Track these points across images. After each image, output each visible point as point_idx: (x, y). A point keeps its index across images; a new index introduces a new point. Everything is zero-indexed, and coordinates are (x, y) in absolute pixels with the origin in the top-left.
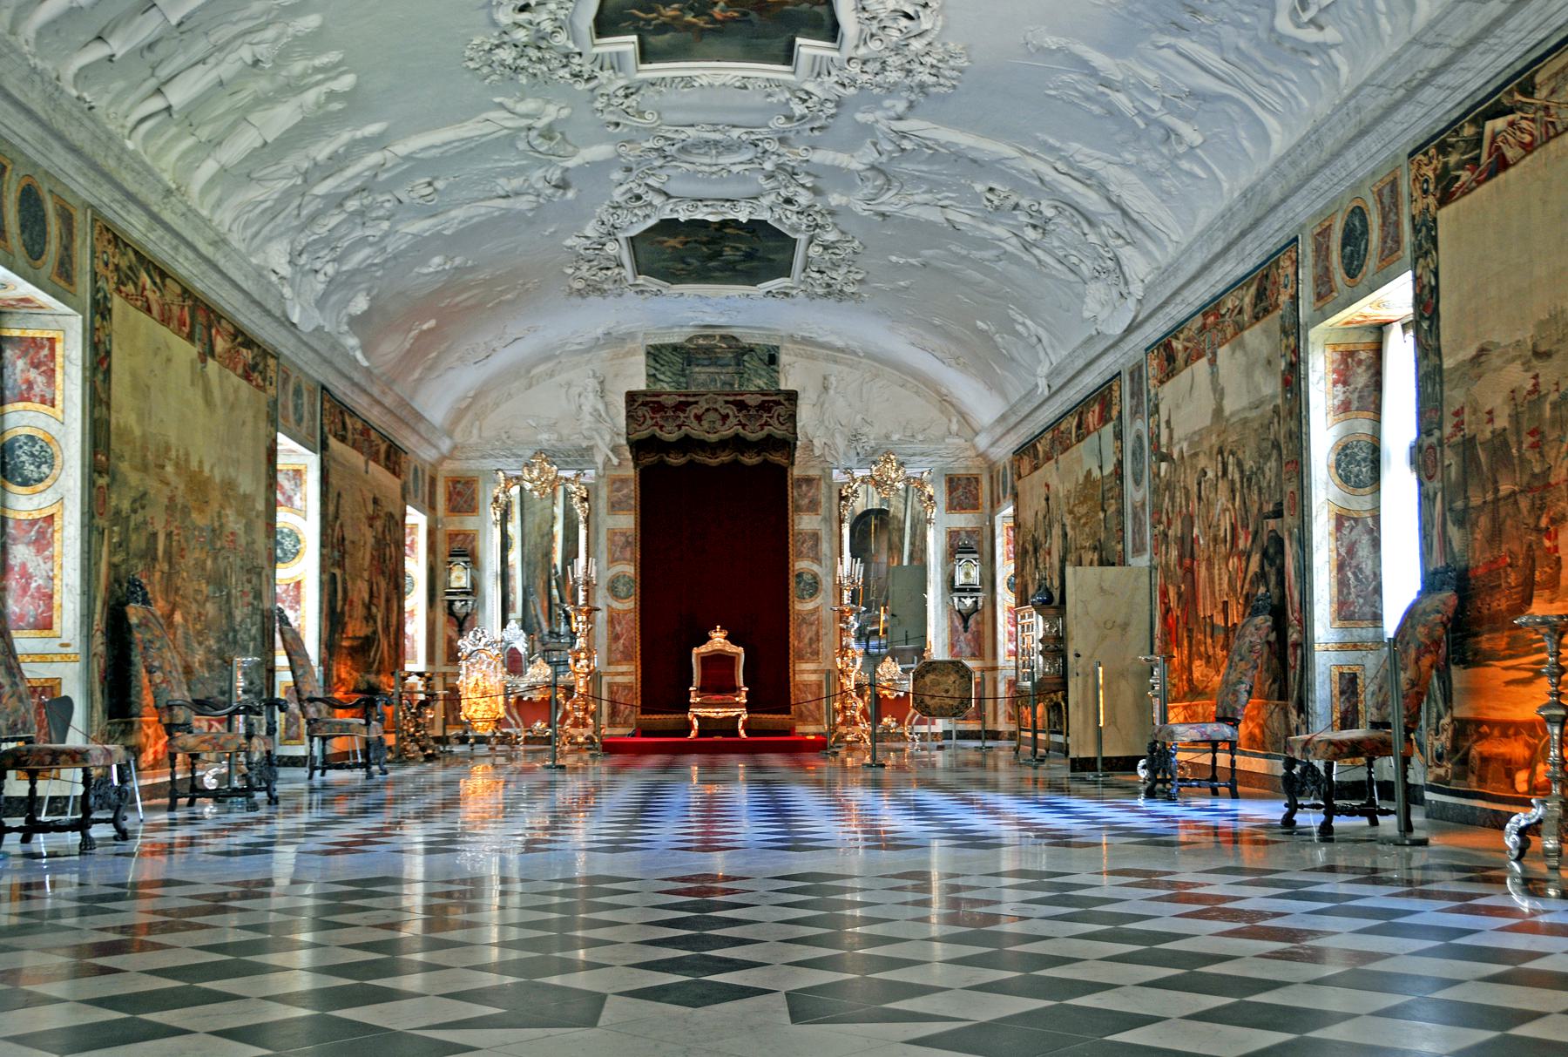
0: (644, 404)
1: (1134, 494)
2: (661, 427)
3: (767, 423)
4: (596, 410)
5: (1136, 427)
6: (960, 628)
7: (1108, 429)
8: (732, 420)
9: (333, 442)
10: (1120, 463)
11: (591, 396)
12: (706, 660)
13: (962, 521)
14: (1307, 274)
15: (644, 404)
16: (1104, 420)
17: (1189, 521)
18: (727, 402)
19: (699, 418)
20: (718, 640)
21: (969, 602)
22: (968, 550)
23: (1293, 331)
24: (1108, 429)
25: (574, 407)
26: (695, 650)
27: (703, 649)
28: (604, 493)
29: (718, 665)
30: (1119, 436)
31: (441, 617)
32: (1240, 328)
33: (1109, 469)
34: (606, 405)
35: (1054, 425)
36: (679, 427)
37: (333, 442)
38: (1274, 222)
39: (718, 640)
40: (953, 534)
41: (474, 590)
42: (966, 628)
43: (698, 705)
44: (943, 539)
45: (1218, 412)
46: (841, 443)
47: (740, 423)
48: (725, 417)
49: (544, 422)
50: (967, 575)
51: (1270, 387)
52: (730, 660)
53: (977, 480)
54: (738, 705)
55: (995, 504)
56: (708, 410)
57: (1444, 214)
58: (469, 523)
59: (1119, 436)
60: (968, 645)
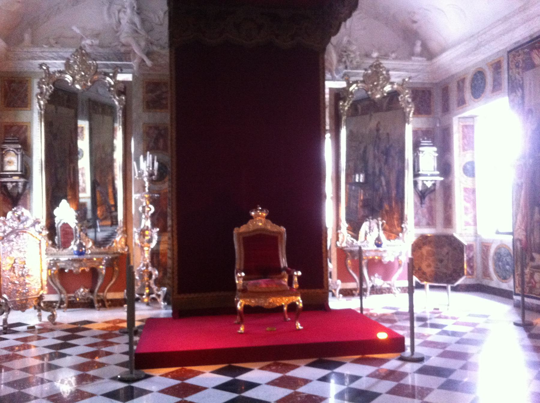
4: (134, 24)
6: (418, 204)
11: (129, 11)
20: (259, 219)
25: (114, 21)
26: (236, 231)
27: (243, 229)
29: (260, 243)
34: (143, 21)
39: (259, 219)
40: (415, 133)
41: (26, 172)
58: (22, 116)
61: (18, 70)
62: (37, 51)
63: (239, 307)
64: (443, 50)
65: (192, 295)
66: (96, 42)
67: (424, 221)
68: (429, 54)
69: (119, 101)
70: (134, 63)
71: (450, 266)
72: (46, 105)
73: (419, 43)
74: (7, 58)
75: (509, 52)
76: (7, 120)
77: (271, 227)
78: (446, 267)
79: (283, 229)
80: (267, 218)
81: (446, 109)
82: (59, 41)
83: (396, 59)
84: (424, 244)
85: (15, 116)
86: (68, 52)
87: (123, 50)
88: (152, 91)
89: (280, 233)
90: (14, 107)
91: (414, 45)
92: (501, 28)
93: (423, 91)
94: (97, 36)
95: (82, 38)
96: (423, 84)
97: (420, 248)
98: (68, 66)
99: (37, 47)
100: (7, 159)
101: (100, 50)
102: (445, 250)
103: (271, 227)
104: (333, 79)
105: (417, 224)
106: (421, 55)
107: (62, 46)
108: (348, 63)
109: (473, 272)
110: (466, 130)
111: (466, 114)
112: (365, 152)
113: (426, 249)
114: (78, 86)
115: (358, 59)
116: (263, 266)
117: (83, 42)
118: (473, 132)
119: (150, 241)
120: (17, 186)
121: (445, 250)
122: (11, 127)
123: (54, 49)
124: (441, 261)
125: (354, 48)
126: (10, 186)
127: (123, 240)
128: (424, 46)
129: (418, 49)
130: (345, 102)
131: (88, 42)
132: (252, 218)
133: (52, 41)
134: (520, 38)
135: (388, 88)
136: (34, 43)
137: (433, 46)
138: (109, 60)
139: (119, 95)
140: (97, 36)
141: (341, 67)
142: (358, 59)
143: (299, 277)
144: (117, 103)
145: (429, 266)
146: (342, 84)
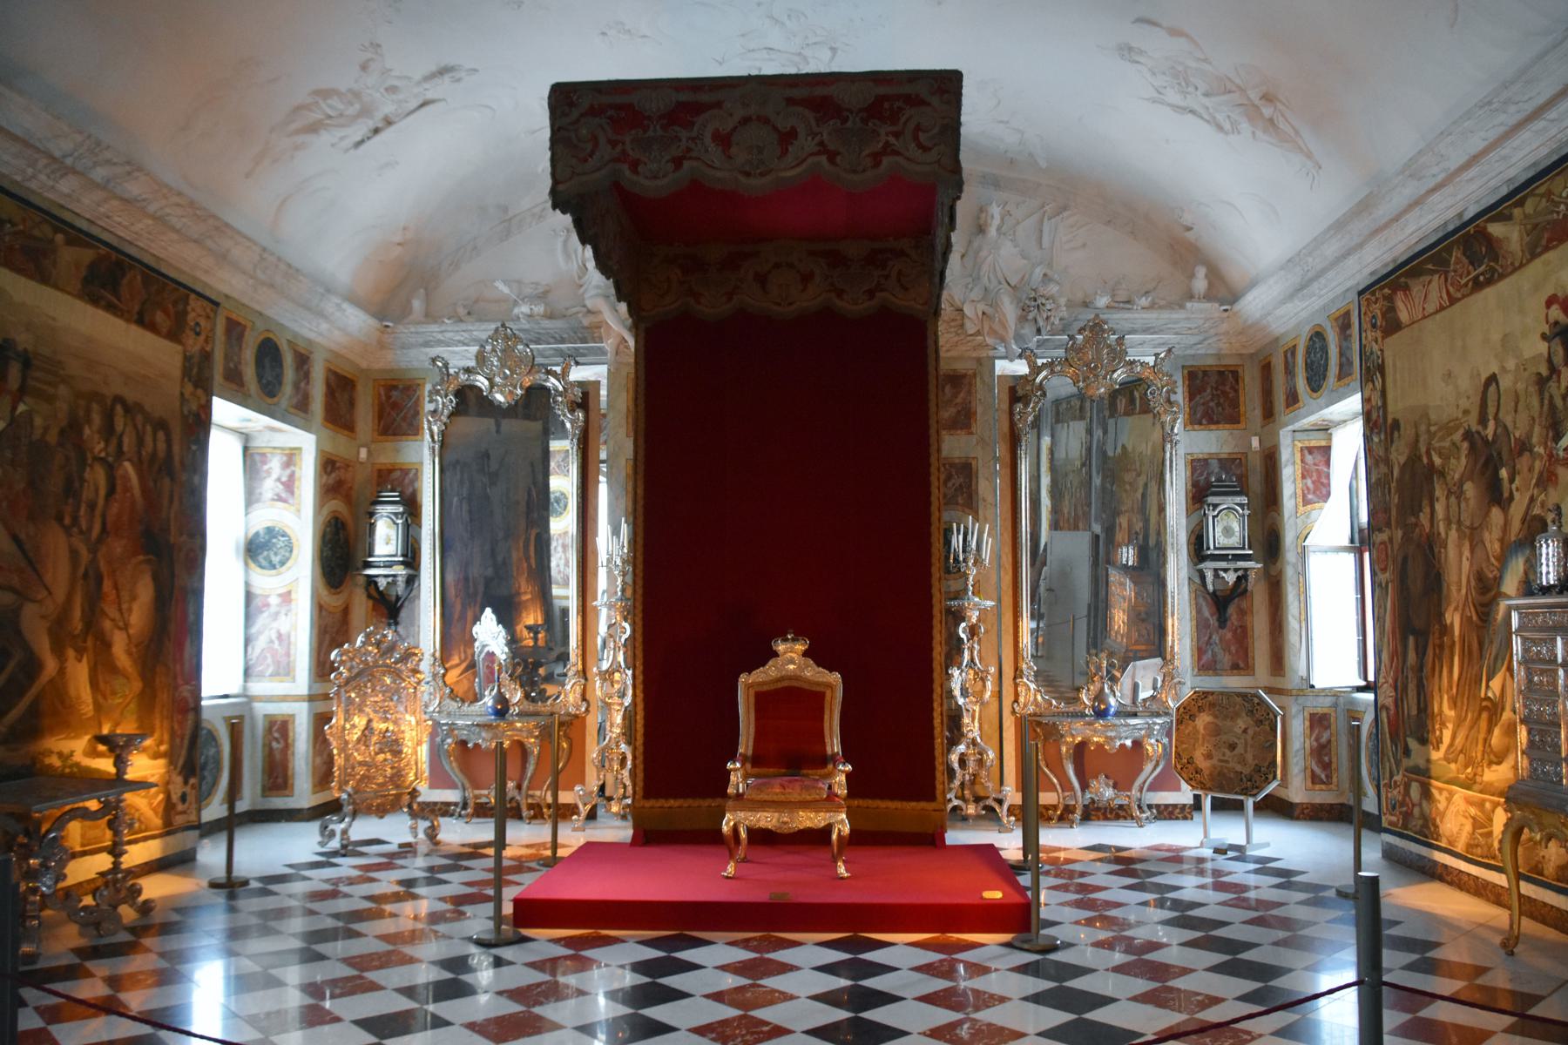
0: (593, 112)
2: (634, 166)
3: (888, 150)
6: (1213, 621)
8: (805, 144)
12: (766, 701)
13: (1210, 442)
15: (593, 112)
18: (791, 101)
19: (724, 140)
20: (792, 658)
21: (1231, 578)
26: (743, 678)
29: (790, 708)
36: (678, 162)
39: (792, 658)
40: (1197, 465)
41: (411, 558)
42: (1222, 622)
46: (1010, 311)
47: (823, 149)
48: (787, 137)
49: (528, 291)
53: (1235, 374)
56: (746, 121)
60: (1226, 649)
61: (403, 365)
63: (725, 829)
64: (1253, 284)
65: (672, 802)
66: (539, 309)
67: (1225, 660)
68: (1224, 292)
69: (572, 422)
71: (1249, 757)
72: (443, 433)
73: (1201, 272)
74: (382, 345)
75: (1360, 293)
76: (384, 460)
78: (1243, 761)
79: (835, 678)
80: (805, 654)
81: (1269, 413)
82: (473, 311)
83: (1152, 307)
84: (1200, 709)
85: (398, 451)
86: (484, 330)
87: (586, 322)
89: (829, 686)
90: (394, 435)
91: (1192, 276)
92: (1332, 249)
93: (1221, 373)
94: (543, 296)
95: (516, 303)
96: (1218, 356)
97: (1192, 717)
98: (481, 358)
99: (435, 322)
101: (547, 324)
102: (1241, 723)
103: (814, 673)
104: (1008, 357)
105: (1205, 665)
106: (1209, 297)
107: (480, 320)
108: (1041, 323)
109: (1329, 777)
110: (1309, 458)
111: (1307, 422)
112: (1144, 495)
113: (1203, 720)
114: (499, 397)
115: (1064, 312)
116: (790, 749)
117: (516, 311)
118: (1328, 463)
119: (623, 695)
120: (394, 583)
121: (1241, 723)
122: (390, 471)
123: (463, 326)
124: (1232, 747)
125: (1053, 289)
126: (382, 583)
127: (578, 689)
128: (1215, 274)
129: (1200, 284)
130: (1026, 405)
131: (525, 309)
132: (776, 654)
133: (462, 311)
134: (1377, 265)
135: (1120, 375)
136: (430, 317)
137: (1234, 275)
138: (563, 341)
139: (572, 411)
141: (1028, 330)
142: (1064, 312)
143: (848, 776)
144: (568, 425)
145: (1209, 756)
146: (1021, 368)
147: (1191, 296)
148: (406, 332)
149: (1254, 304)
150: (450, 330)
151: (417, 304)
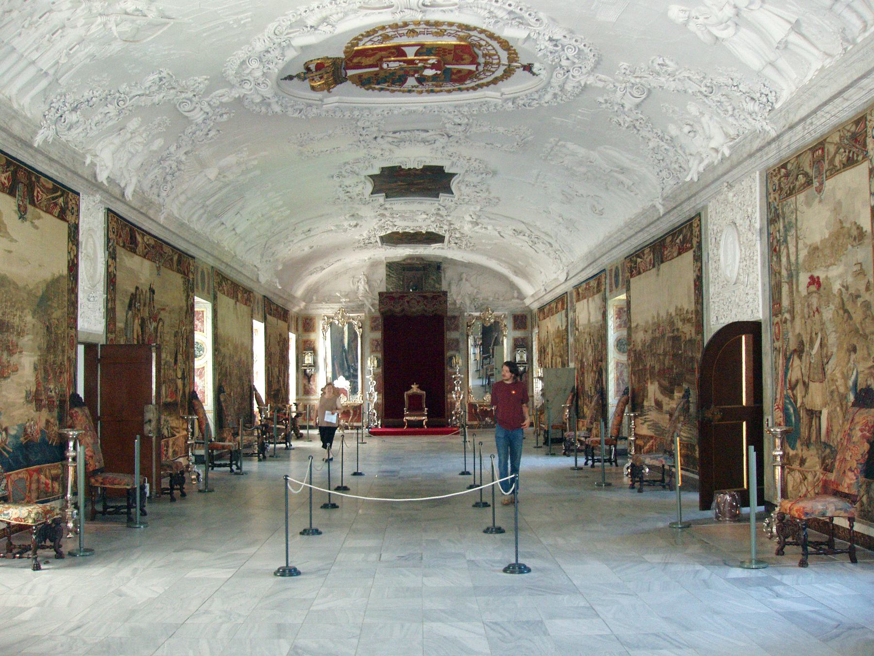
1: (571, 340)
5: (571, 314)
7: (564, 311)
9: (268, 316)
10: (567, 326)
12: (410, 397)
13: (519, 334)
14: (608, 281)
16: (563, 309)
17: (583, 356)
19: (408, 302)
20: (415, 388)
22: (522, 346)
23: (605, 300)
24: (564, 311)
28: (368, 323)
29: (414, 398)
30: (567, 316)
31: (301, 376)
32: (594, 294)
33: (564, 327)
34: (369, 287)
35: (549, 304)
37: (268, 316)
38: (599, 262)
39: (415, 388)
41: (315, 364)
43: (407, 415)
44: (511, 342)
45: (589, 320)
46: (468, 302)
48: (418, 302)
50: (521, 357)
51: (600, 318)
52: (419, 397)
54: (424, 415)
55: (532, 327)
57: (632, 280)
59: (567, 316)
62: (320, 305)
70: (366, 310)
77: (419, 391)
82: (329, 299)
88: (374, 322)
100: (306, 357)
103: (419, 391)
106: (518, 298)
126: (308, 371)
129: (516, 295)
140: (346, 296)
147: (513, 298)
148: (311, 306)
149: (528, 302)
150: (324, 305)
151: (314, 298)
